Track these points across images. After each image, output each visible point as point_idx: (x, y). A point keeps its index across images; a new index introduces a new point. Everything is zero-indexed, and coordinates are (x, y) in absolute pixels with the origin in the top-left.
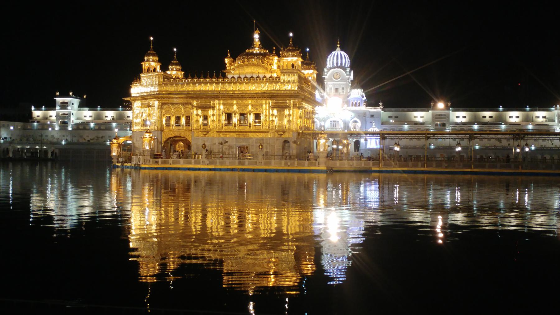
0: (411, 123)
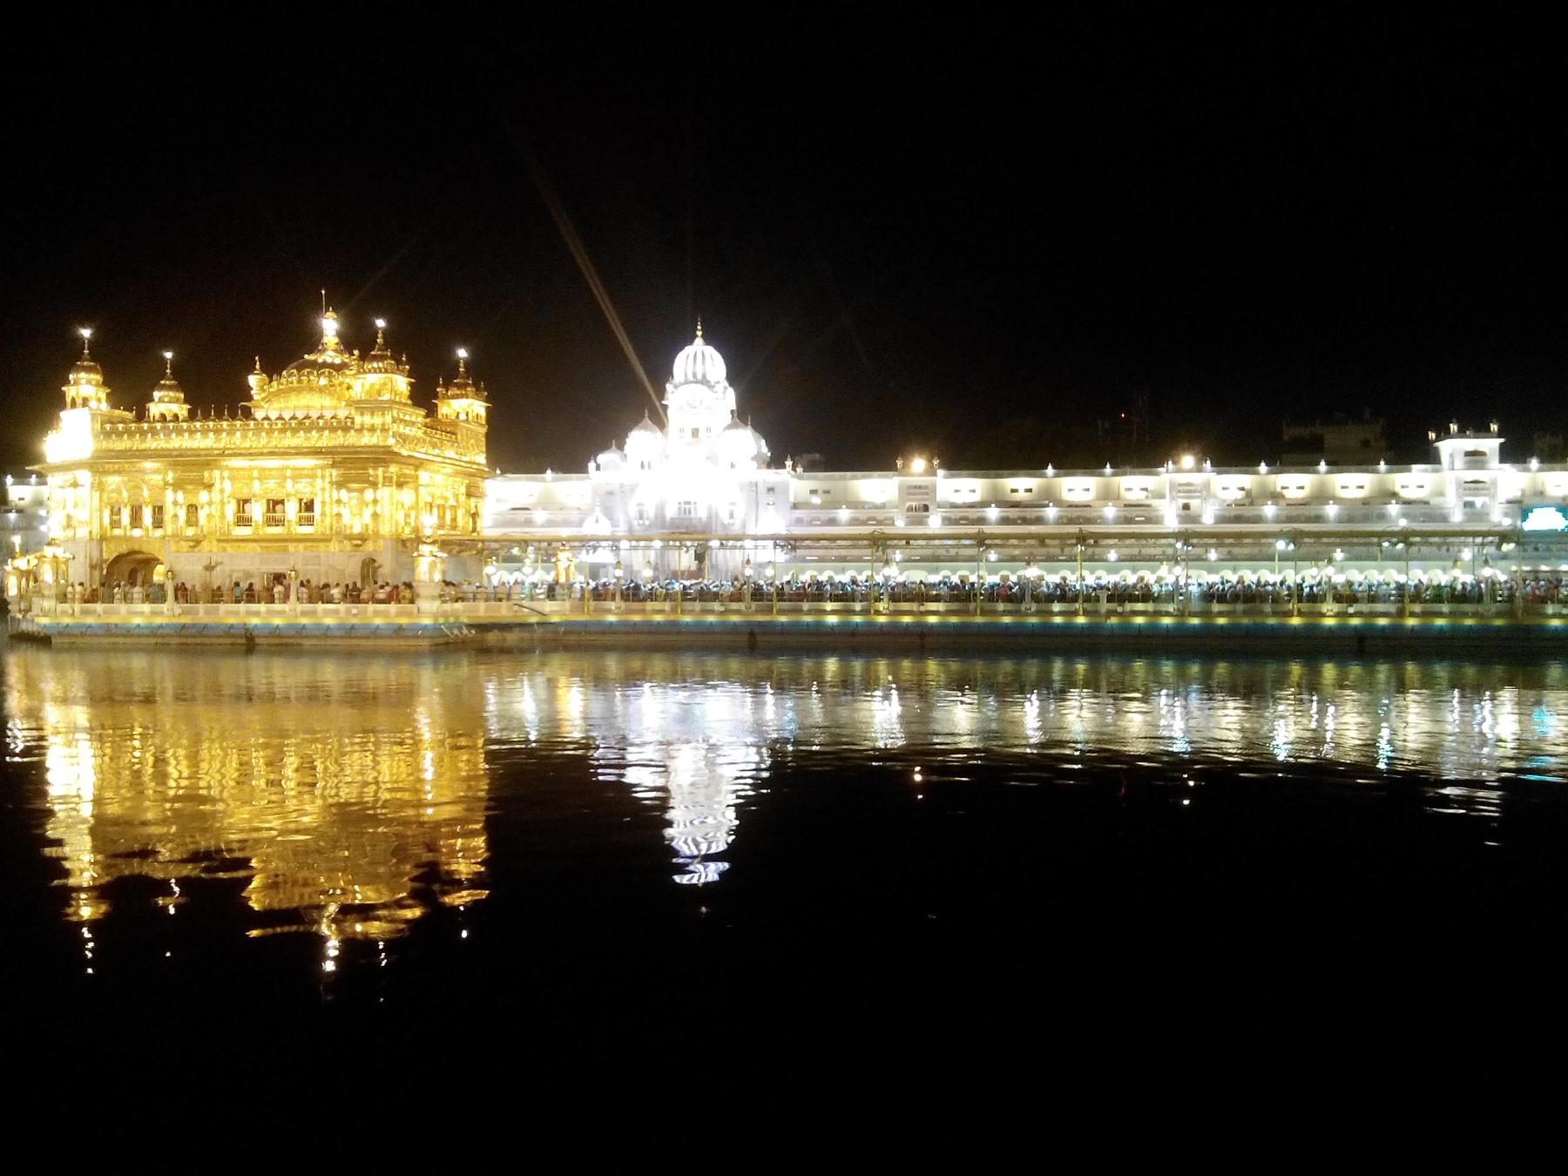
0: (855, 505)
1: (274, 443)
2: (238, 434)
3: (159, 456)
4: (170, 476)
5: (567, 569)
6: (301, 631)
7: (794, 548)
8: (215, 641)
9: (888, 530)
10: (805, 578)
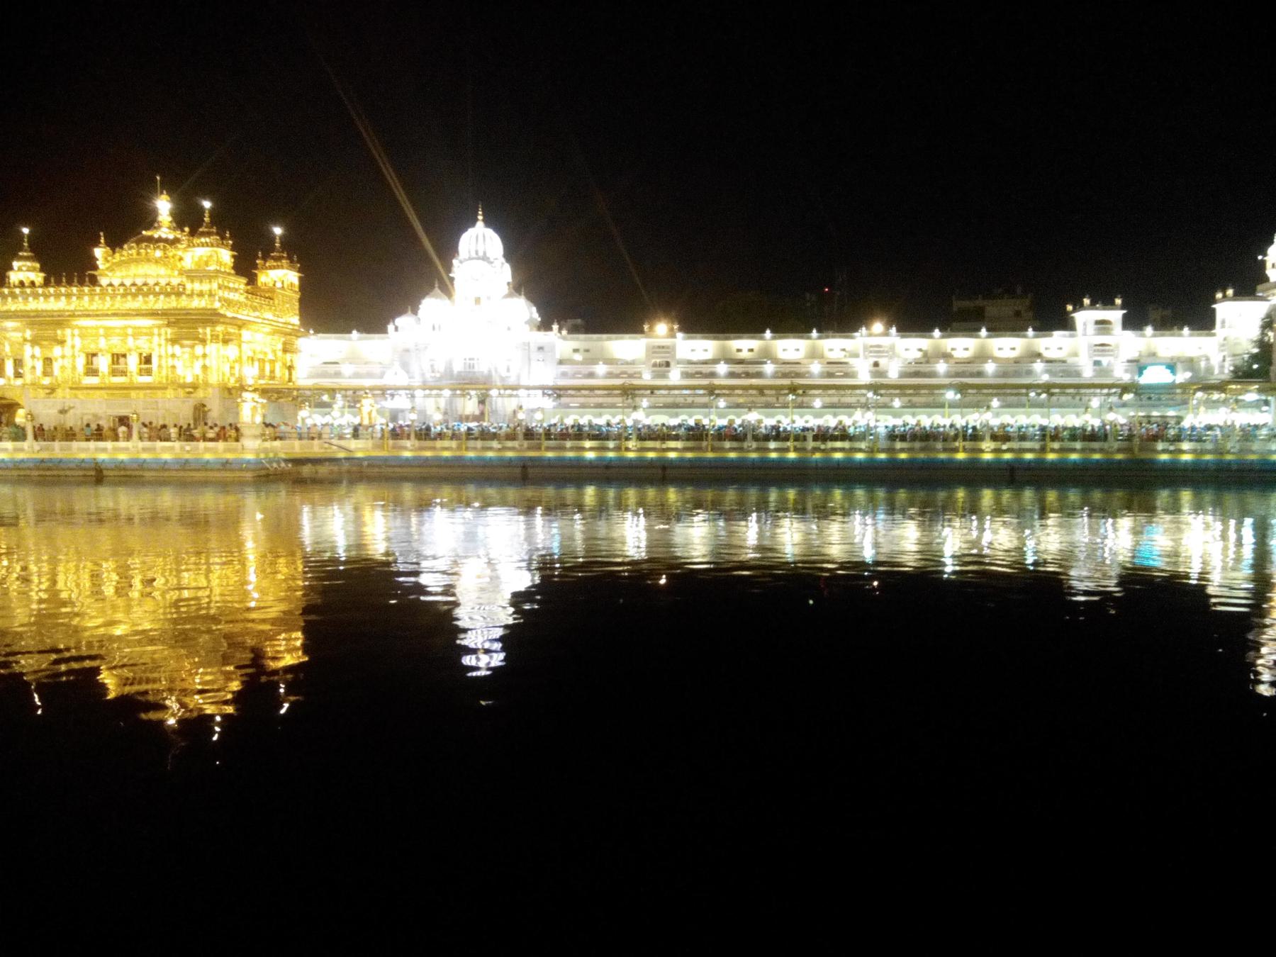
0: (610, 361)
1: (117, 306)
2: (86, 298)
3: (18, 317)
4: (28, 334)
5: (370, 414)
6: (142, 465)
7: (559, 396)
8: (68, 473)
9: (636, 382)
10: (569, 421)
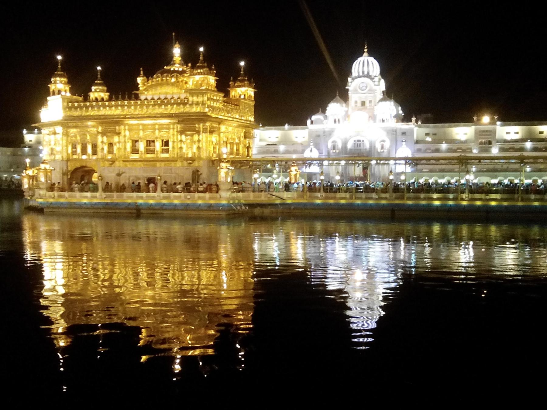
1: (150, 112)
2: (133, 107)
3: (95, 119)
4: (100, 129)
5: (295, 176)
6: (163, 207)
7: (416, 164)
8: (122, 211)
9: (468, 155)
10: (422, 181)
